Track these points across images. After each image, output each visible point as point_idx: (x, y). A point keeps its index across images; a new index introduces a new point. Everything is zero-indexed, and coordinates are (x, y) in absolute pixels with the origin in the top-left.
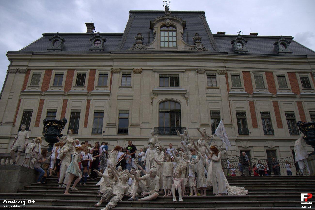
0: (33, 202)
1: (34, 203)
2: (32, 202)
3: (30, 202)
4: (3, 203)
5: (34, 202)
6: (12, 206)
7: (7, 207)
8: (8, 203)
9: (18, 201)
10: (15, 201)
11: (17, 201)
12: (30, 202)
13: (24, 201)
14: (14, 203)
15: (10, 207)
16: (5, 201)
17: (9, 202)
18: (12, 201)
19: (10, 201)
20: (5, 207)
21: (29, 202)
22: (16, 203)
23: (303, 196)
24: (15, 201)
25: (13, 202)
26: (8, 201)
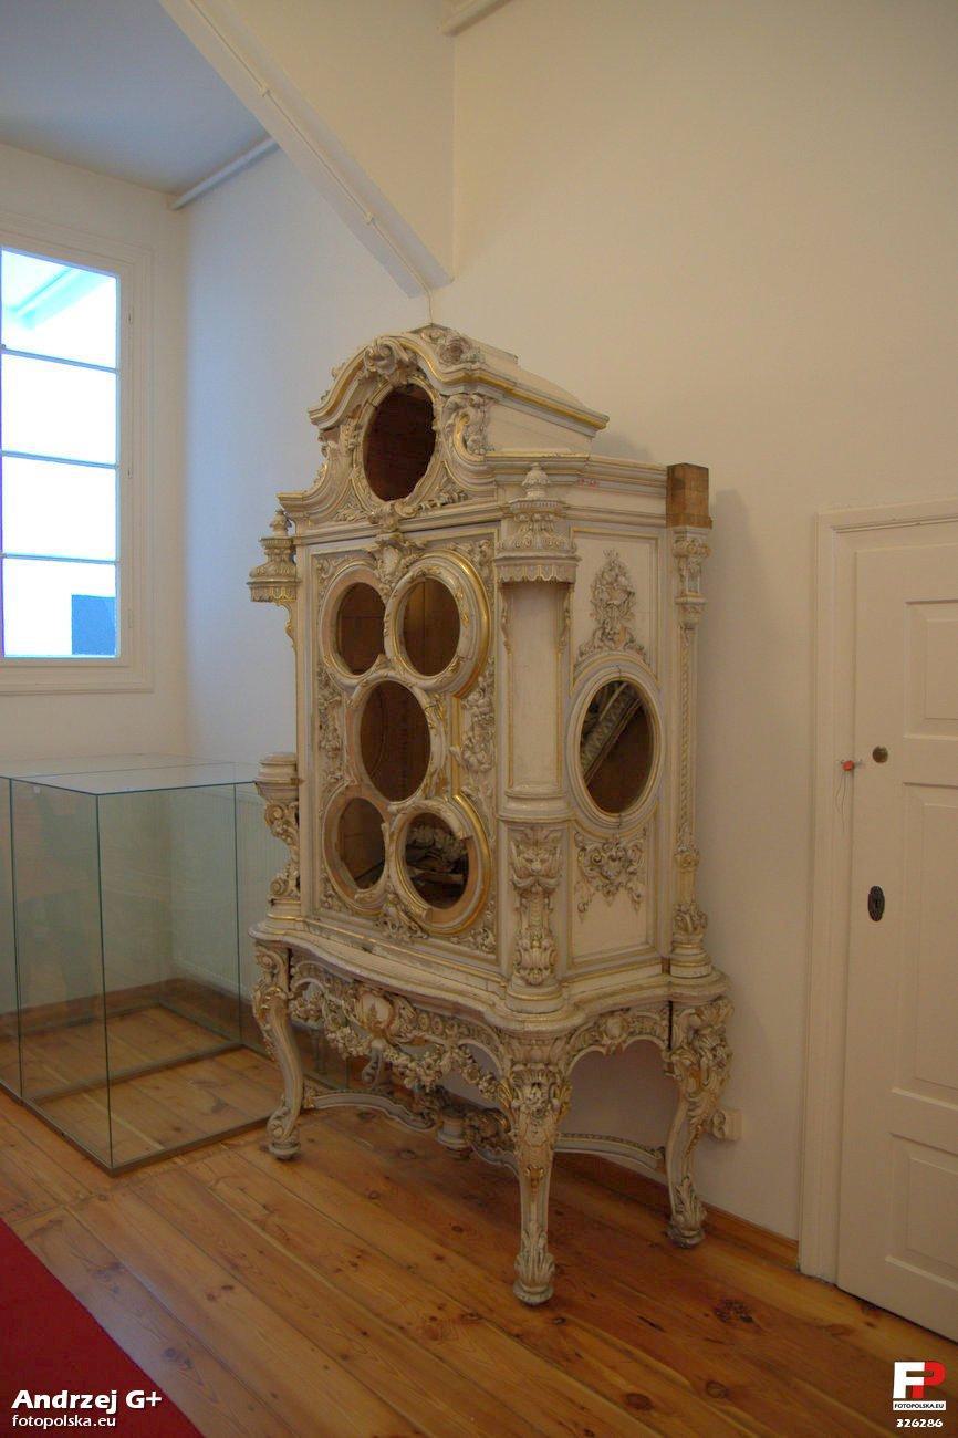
0: (150, 1402)
1: (153, 1404)
2: (147, 1404)
3: (138, 1400)
4: (15, 1405)
5: (157, 1402)
6: (53, 1422)
7: (33, 1421)
8: (37, 1406)
9: (83, 1397)
10: (69, 1399)
11: (78, 1397)
12: (137, 1403)
13: (110, 1396)
14: (64, 1405)
15: (44, 1423)
16: (23, 1397)
17: (42, 1402)
18: (56, 1398)
19: (46, 1398)
20: (23, 1422)
21: (134, 1401)
22: (73, 1406)
23: (905, 1375)
24: (69, 1399)
25: (60, 1401)
26: (38, 1398)
